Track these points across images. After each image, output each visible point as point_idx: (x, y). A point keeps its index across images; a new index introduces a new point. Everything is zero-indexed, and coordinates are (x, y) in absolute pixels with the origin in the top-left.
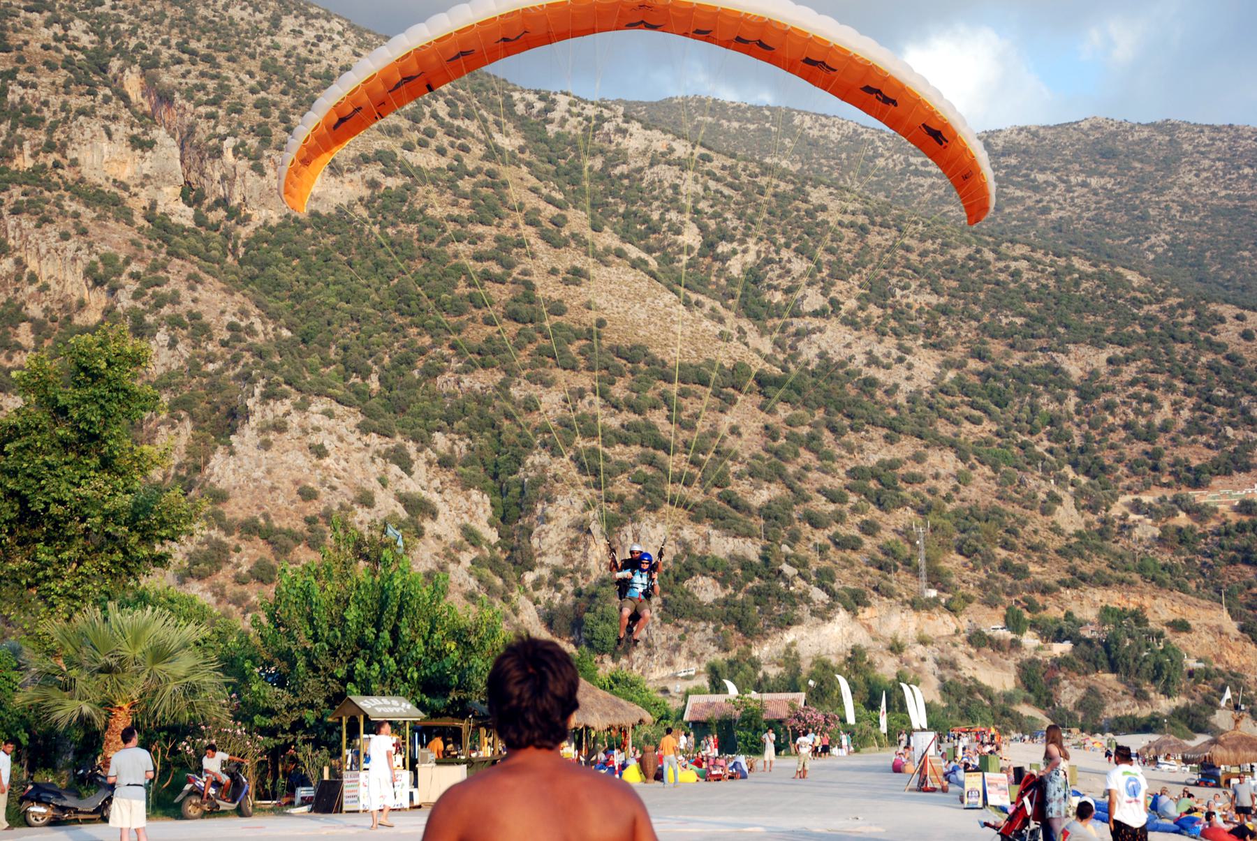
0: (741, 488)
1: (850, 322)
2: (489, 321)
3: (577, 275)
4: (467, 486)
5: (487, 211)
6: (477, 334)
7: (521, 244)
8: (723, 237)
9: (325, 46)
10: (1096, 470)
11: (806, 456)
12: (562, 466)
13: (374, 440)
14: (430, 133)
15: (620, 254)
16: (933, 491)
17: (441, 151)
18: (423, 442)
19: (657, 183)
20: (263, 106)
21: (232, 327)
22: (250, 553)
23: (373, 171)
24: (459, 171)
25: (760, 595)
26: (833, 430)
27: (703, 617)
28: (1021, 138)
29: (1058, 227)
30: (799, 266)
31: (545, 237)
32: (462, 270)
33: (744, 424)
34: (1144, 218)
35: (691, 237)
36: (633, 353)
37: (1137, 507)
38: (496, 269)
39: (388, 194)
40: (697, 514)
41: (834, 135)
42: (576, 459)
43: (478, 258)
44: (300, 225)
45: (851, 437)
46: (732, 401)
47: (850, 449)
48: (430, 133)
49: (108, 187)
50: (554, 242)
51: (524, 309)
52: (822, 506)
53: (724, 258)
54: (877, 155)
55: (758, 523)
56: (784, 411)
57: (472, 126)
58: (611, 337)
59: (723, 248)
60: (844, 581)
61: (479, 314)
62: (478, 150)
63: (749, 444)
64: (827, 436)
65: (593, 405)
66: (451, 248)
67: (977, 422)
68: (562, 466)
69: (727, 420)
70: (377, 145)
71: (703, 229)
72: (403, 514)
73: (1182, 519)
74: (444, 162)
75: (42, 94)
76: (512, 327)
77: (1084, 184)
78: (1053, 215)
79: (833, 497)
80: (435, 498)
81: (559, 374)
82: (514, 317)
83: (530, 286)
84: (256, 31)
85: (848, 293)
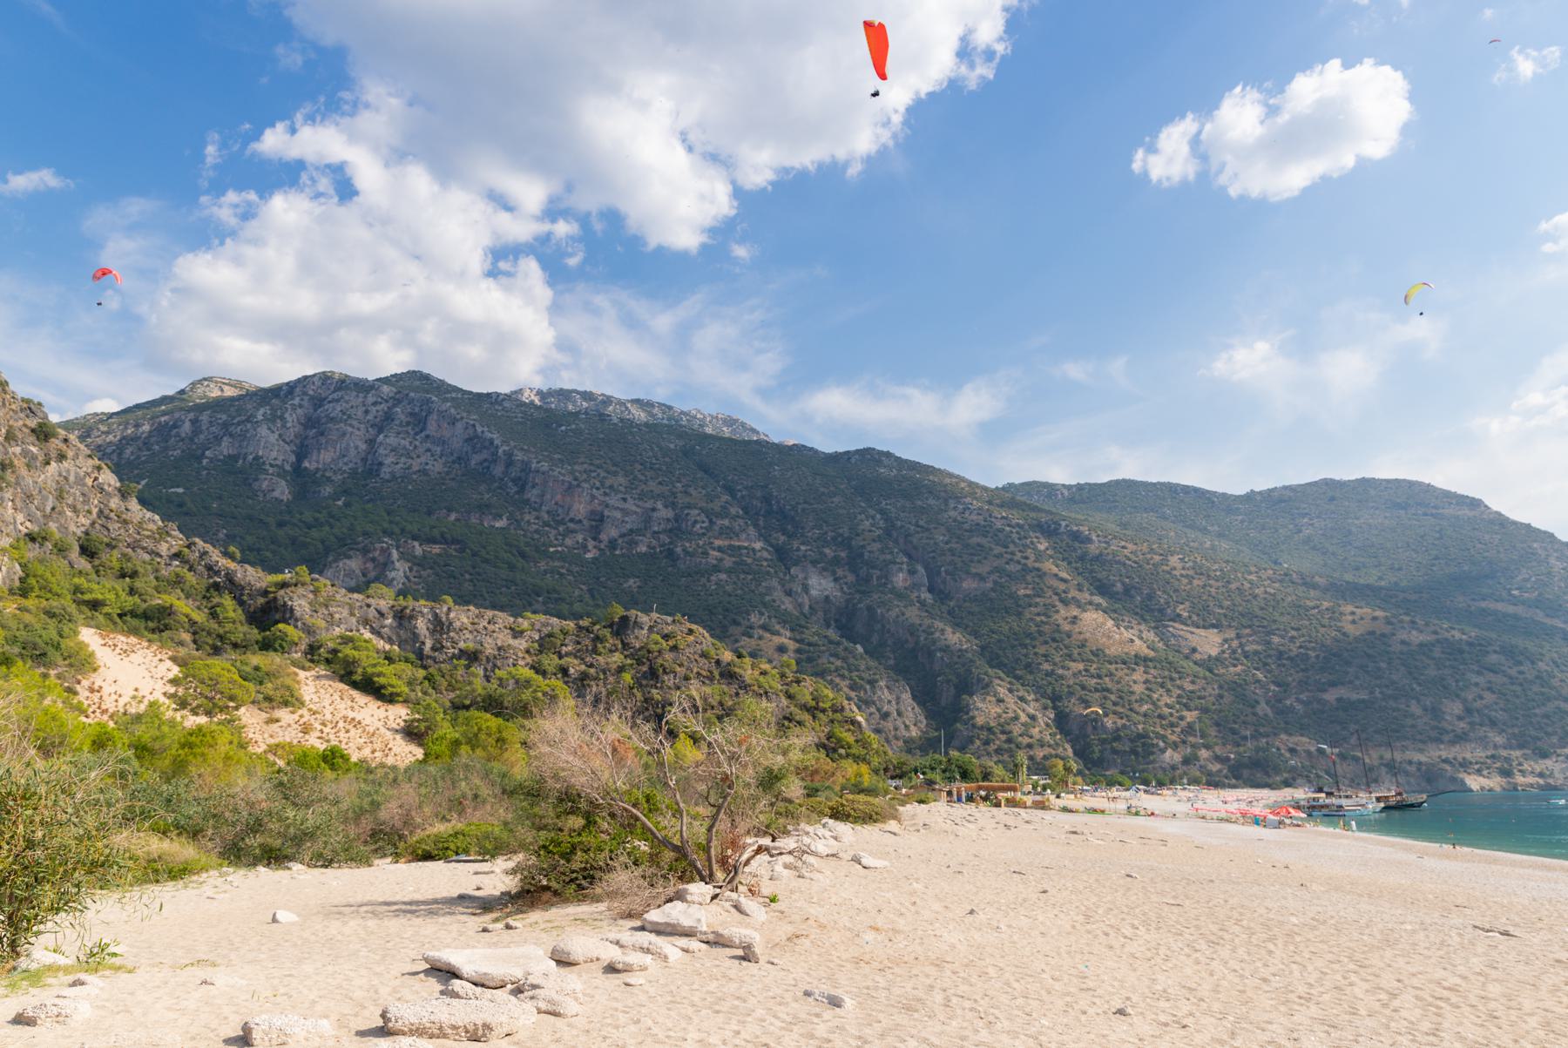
0: (1136, 706)
6: (1041, 650)
14: (1013, 553)
15: (1090, 603)
20: (950, 550)
23: (995, 577)
26: (1172, 679)
31: (1062, 601)
50: (1065, 602)
52: (1166, 711)
63: (1139, 689)
73: (1315, 705)
74: (1019, 567)
81: (1072, 664)
82: (1054, 640)
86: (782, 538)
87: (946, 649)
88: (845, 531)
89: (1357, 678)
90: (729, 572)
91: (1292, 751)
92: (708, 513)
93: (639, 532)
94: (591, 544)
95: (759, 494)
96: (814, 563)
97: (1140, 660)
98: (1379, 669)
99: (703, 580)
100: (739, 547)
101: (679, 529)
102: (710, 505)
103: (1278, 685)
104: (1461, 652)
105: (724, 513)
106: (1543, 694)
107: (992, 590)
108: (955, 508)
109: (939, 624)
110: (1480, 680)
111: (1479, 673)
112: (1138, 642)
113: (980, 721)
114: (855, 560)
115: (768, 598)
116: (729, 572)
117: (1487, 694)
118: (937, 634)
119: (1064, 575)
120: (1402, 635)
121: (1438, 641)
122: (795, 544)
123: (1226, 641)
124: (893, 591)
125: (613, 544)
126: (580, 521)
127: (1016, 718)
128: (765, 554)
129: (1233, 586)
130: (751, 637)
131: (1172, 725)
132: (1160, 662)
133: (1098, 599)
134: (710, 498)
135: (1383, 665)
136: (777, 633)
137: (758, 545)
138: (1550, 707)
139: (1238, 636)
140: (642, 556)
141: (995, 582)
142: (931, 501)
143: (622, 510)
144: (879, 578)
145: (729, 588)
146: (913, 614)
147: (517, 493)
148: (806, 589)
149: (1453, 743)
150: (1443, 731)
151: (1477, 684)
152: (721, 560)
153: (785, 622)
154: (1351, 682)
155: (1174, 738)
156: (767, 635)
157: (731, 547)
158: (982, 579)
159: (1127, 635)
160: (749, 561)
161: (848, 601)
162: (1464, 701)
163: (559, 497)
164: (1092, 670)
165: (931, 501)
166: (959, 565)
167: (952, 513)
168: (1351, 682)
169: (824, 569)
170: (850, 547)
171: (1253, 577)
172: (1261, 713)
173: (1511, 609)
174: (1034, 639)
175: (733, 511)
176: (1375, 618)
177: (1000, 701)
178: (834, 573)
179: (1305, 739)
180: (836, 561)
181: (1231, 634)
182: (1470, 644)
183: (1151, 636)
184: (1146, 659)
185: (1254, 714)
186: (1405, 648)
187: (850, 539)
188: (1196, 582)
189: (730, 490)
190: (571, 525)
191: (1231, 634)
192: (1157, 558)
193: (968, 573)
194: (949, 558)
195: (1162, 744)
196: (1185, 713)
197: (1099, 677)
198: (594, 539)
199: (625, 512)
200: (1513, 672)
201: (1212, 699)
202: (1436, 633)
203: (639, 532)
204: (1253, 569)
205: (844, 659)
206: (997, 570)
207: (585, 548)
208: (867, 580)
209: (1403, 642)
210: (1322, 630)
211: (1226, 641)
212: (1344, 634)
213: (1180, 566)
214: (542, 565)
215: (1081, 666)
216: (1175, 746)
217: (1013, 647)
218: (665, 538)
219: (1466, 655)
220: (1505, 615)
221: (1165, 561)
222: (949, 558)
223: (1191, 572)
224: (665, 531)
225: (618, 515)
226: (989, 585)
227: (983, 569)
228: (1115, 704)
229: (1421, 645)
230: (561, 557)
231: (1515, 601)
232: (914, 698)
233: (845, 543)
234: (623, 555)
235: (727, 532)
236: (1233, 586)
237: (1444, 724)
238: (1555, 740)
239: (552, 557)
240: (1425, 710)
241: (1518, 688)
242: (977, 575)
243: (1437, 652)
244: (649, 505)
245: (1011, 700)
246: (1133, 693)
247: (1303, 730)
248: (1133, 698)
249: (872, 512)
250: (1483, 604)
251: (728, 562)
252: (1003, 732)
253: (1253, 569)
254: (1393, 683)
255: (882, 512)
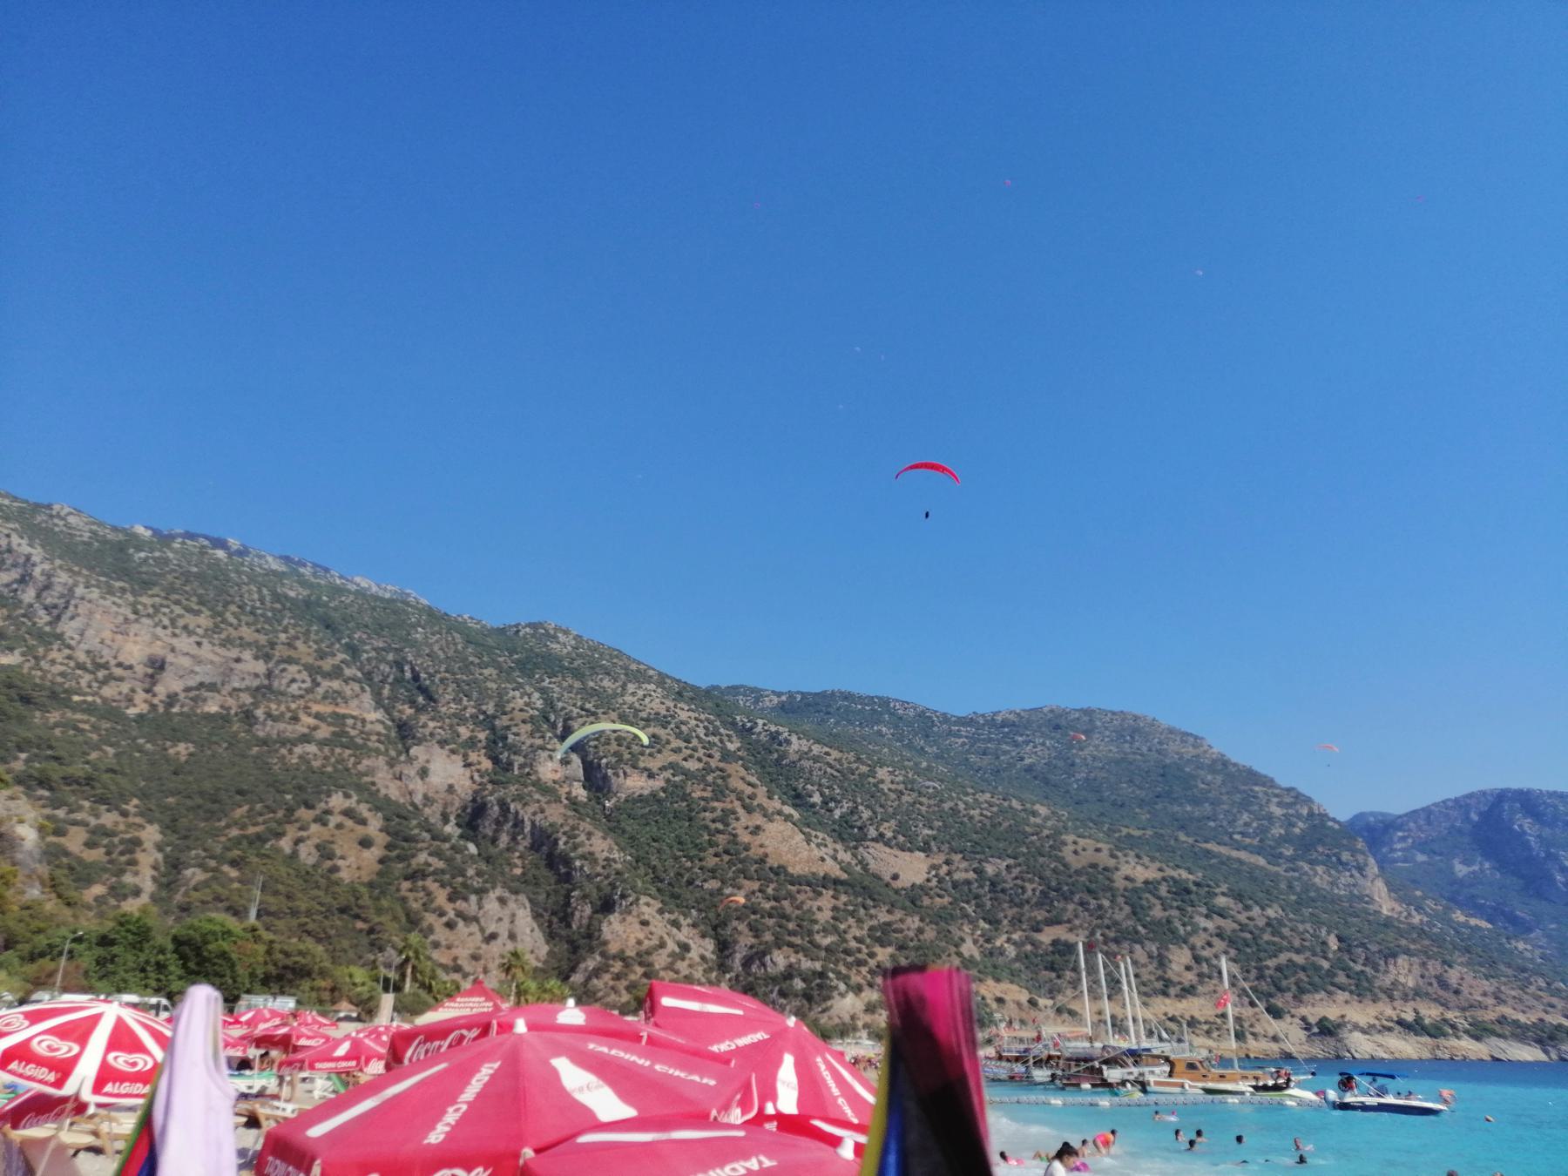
0: (818, 938)
1: (887, 844)
2: (716, 855)
3: (757, 830)
4: (703, 936)
5: (719, 794)
6: (711, 862)
7: (734, 812)
8: (833, 799)
9: (647, 700)
10: (994, 922)
11: (851, 921)
12: (742, 927)
13: (667, 915)
14: (695, 749)
15: (780, 813)
16: (906, 937)
17: (700, 760)
18: (686, 916)
19: (802, 769)
21: (607, 859)
22: (617, 967)
23: (668, 774)
24: (708, 769)
25: (820, 986)
26: (865, 907)
27: (796, 996)
28: (1012, 717)
29: (1029, 769)
30: (866, 814)
31: (744, 807)
32: (706, 827)
33: (823, 906)
34: (1073, 765)
35: (817, 799)
36: (779, 871)
37: (1008, 940)
38: (720, 826)
39: (676, 786)
40: (796, 948)
41: (912, 714)
42: (749, 924)
43: (713, 821)
44: (635, 801)
45: (873, 911)
46: (820, 894)
47: (871, 917)
48: (695, 749)
49: (550, 784)
50: (749, 810)
51: (734, 850)
52: (853, 944)
53: (830, 811)
54: (934, 725)
55: (823, 954)
56: (844, 898)
57: (716, 739)
58: (772, 862)
59: (832, 805)
60: (856, 979)
61: (711, 851)
62: (717, 755)
63: (825, 916)
64: (862, 911)
65: (758, 898)
66: (703, 814)
67: (939, 896)
68: (742, 927)
69: (818, 903)
70: (671, 759)
71: (822, 795)
72: (677, 950)
73: (1029, 947)
74: (701, 766)
75: (522, 738)
76: (726, 858)
77: (1043, 744)
78: (1027, 761)
79: (859, 940)
80: (691, 942)
81: (746, 882)
82: (727, 852)
83: (735, 836)
84: (615, 695)
85: (888, 830)
86: (409, 711)
87: (590, 857)
88: (490, 708)
89: (1076, 916)
90: (322, 743)
91: (1000, 1001)
92: (313, 671)
93: (212, 687)
94: (140, 696)
95: (390, 657)
96: (442, 743)
97: (828, 882)
98: (1100, 907)
99: (284, 751)
100: (344, 717)
101: (269, 688)
102: (320, 663)
103: (990, 923)
104: (1188, 892)
105: (336, 673)
106: (1274, 944)
107: (664, 790)
108: (633, 694)
109: (586, 825)
110: (1209, 925)
111: (1207, 916)
112: (829, 861)
113: (613, 948)
114: (497, 744)
115: (367, 779)
116: (322, 743)
117: (1216, 941)
118: (583, 837)
119: (753, 780)
120: (1126, 870)
121: (1164, 879)
122: (423, 718)
123: (933, 867)
124: (538, 784)
125: (172, 699)
126: (130, 667)
127: (662, 945)
128: (380, 728)
129: (946, 806)
130: (325, 824)
131: (860, 963)
132: (852, 886)
133: (788, 810)
134: (322, 655)
135: (1106, 903)
136: (363, 822)
137: (372, 716)
138: (1283, 958)
139: (947, 862)
140: (208, 717)
141: (668, 781)
142: (606, 683)
143: (193, 657)
144: (522, 767)
145: (316, 764)
146: (555, 814)
147: (50, 623)
148: (424, 773)
149: (1179, 997)
150: (1168, 983)
151: (1205, 930)
152: (315, 728)
153: (378, 809)
154: (1069, 921)
155: (859, 979)
156: (349, 823)
157: (335, 714)
158: (651, 776)
159: (817, 853)
160: (353, 733)
161: (476, 792)
162: (1193, 948)
163: (107, 634)
164: (770, 891)
165: (606, 683)
166: (627, 756)
167: (629, 699)
168: (1069, 921)
169: (453, 752)
170: (493, 729)
171: (970, 799)
172: (966, 954)
173: (1235, 854)
174: (702, 850)
175: (348, 672)
176: (1098, 850)
177: (645, 923)
178: (465, 756)
179: (1014, 987)
180: (472, 743)
181: (939, 859)
182: (1197, 884)
183: (846, 856)
184: (837, 882)
185: (959, 954)
186: (1130, 885)
187: (494, 717)
188: (905, 798)
189: (354, 651)
190: (118, 672)
191: (939, 859)
192: (864, 769)
193: (634, 767)
194: (614, 747)
195: (842, 987)
196: (878, 949)
197: (776, 899)
198: (147, 691)
199: (198, 660)
200: (1242, 918)
201: (911, 934)
202: (1160, 870)
203: (212, 687)
204: (970, 790)
205: (449, 861)
206: (672, 766)
207: (130, 700)
208: (509, 766)
209: (1127, 878)
210: (1041, 860)
211: (933, 867)
212: (1065, 865)
213: (888, 779)
214: (54, 717)
215: (756, 885)
216: (858, 989)
217: (676, 858)
218: (247, 699)
219: (1193, 897)
220: (1229, 858)
221: (872, 773)
222: (614, 747)
223: (901, 787)
224: (247, 689)
225: (186, 662)
226: (658, 783)
227: (654, 765)
228: (791, 933)
229: (1146, 882)
230: (89, 709)
231: (1239, 847)
232: (537, 916)
233: (488, 722)
234: (181, 714)
235: (333, 697)
236: (946, 806)
237: (1170, 974)
238: (1288, 996)
239: (75, 708)
240: (1151, 957)
241: (1248, 936)
242: (645, 769)
243: (1163, 890)
244: (234, 653)
245: (659, 926)
246: (816, 922)
247: (1014, 976)
248: (816, 927)
249: (528, 689)
250: (1209, 846)
251: (324, 732)
252: (641, 964)
253: (970, 790)
254: (1116, 923)
255: (543, 691)
